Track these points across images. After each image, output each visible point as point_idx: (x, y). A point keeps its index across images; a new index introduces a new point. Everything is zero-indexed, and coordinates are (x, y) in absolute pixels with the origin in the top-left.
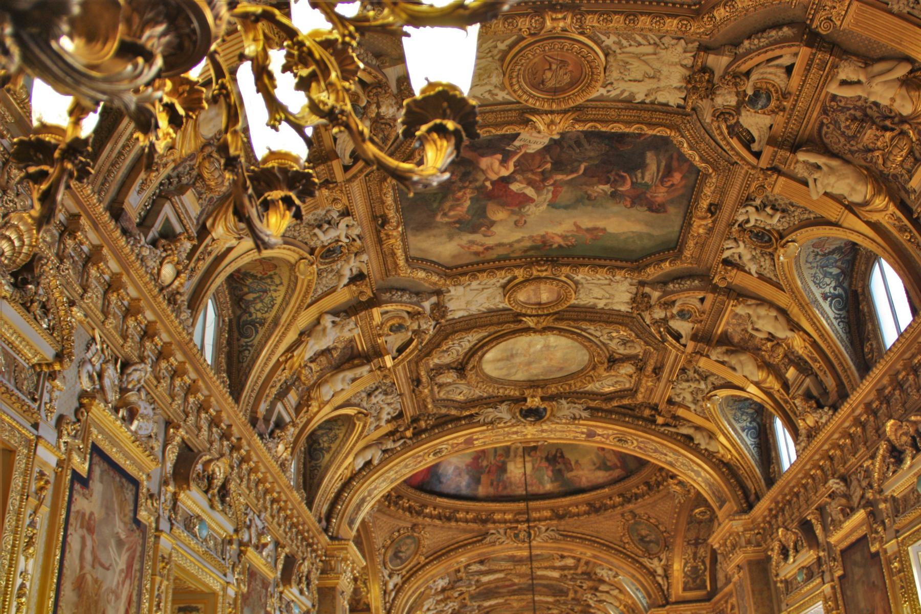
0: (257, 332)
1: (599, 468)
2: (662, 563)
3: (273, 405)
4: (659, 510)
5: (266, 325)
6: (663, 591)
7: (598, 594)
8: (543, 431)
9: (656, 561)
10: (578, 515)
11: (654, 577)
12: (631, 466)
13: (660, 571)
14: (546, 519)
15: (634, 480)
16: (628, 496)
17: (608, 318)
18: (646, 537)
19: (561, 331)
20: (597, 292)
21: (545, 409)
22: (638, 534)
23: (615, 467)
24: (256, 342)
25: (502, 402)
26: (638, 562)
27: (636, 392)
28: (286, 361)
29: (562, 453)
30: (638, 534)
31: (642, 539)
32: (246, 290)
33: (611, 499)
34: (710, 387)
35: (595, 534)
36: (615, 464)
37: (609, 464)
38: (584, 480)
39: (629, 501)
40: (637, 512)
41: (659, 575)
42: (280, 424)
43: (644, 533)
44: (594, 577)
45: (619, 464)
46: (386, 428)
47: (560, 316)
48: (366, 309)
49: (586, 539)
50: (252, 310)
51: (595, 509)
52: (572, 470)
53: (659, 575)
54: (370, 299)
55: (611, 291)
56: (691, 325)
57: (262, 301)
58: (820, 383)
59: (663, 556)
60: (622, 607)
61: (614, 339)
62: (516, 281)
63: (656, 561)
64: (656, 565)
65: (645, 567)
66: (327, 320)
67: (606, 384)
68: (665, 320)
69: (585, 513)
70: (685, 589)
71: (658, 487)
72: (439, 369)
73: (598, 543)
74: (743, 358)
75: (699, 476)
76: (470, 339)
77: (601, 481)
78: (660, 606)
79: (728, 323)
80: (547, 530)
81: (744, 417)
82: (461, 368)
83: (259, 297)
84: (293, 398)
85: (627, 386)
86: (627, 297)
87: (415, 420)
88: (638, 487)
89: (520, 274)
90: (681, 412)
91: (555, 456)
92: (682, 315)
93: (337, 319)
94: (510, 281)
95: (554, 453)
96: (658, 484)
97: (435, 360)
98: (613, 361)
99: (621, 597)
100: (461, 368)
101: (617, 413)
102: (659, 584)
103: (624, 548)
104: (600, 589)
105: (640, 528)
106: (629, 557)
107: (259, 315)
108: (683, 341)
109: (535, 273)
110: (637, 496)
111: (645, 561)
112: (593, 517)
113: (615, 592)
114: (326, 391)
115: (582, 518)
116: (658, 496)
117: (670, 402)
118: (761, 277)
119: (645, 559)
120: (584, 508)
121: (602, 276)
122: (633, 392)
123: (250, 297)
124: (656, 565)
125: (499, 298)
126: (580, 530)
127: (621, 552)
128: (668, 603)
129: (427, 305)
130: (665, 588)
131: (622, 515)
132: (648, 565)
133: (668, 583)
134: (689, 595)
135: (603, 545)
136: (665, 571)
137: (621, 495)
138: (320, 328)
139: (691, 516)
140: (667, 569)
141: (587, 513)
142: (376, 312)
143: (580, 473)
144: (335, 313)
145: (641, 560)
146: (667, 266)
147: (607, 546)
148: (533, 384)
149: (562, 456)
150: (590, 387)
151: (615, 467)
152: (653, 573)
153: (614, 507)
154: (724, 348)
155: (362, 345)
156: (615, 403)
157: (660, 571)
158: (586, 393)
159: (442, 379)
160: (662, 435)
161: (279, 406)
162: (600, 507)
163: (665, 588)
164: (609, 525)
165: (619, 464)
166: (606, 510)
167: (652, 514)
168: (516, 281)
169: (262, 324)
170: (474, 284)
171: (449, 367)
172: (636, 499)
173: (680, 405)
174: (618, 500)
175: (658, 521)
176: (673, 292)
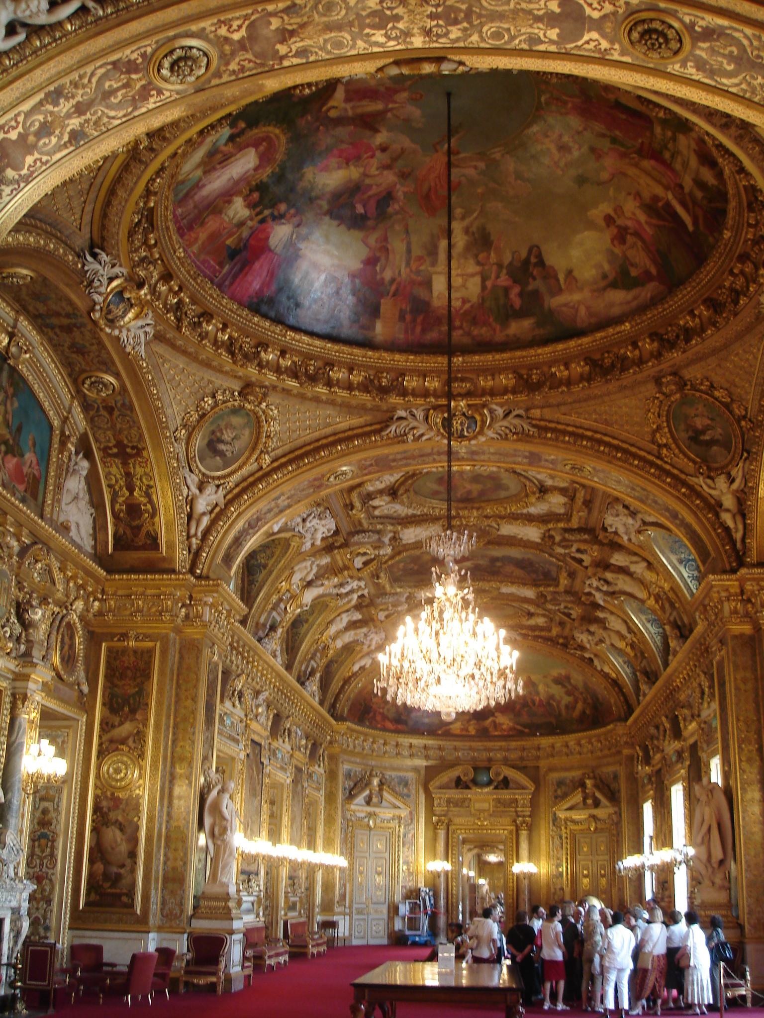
1: (614, 285)
2: (735, 486)
6: (733, 542)
7: (609, 576)
9: (721, 482)
10: (569, 382)
11: (717, 516)
14: (505, 391)
15: (685, 294)
16: (671, 336)
18: (703, 432)
22: (689, 427)
23: (647, 277)
26: (684, 484)
29: (539, 256)
30: (689, 427)
31: (695, 437)
33: (635, 345)
35: (601, 427)
36: (647, 273)
37: (634, 272)
38: (583, 311)
39: (672, 345)
40: (687, 374)
41: (728, 510)
43: (699, 423)
44: (601, 537)
45: (654, 271)
49: (583, 437)
52: (560, 291)
53: (728, 510)
59: (737, 472)
60: (651, 602)
63: (721, 482)
64: (722, 490)
65: (699, 495)
69: (582, 378)
71: (736, 302)
73: (607, 444)
77: (616, 311)
78: (724, 572)
80: (506, 415)
88: (691, 313)
91: (526, 262)
95: (524, 254)
96: (736, 294)
99: (650, 576)
102: (727, 529)
103: (659, 457)
104: (613, 561)
105: (691, 412)
106: (668, 474)
110: (688, 334)
111: (700, 482)
112: (598, 387)
113: (639, 568)
115: (575, 389)
116: (736, 325)
119: (701, 480)
126: (573, 418)
127: (652, 464)
128: (741, 564)
130: (738, 536)
131: (658, 381)
133: (745, 526)
135: (617, 448)
143: (576, 297)
145: (692, 480)
147: (625, 451)
149: (541, 263)
151: (647, 277)
152: (715, 507)
157: (729, 502)
162: (613, 366)
163: (738, 536)
164: (630, 408)
165: (654, 271)
166: (623, 370)
167: (717, 379)
172: (688, 340)
174: (648, 346)
175: (730, 394)
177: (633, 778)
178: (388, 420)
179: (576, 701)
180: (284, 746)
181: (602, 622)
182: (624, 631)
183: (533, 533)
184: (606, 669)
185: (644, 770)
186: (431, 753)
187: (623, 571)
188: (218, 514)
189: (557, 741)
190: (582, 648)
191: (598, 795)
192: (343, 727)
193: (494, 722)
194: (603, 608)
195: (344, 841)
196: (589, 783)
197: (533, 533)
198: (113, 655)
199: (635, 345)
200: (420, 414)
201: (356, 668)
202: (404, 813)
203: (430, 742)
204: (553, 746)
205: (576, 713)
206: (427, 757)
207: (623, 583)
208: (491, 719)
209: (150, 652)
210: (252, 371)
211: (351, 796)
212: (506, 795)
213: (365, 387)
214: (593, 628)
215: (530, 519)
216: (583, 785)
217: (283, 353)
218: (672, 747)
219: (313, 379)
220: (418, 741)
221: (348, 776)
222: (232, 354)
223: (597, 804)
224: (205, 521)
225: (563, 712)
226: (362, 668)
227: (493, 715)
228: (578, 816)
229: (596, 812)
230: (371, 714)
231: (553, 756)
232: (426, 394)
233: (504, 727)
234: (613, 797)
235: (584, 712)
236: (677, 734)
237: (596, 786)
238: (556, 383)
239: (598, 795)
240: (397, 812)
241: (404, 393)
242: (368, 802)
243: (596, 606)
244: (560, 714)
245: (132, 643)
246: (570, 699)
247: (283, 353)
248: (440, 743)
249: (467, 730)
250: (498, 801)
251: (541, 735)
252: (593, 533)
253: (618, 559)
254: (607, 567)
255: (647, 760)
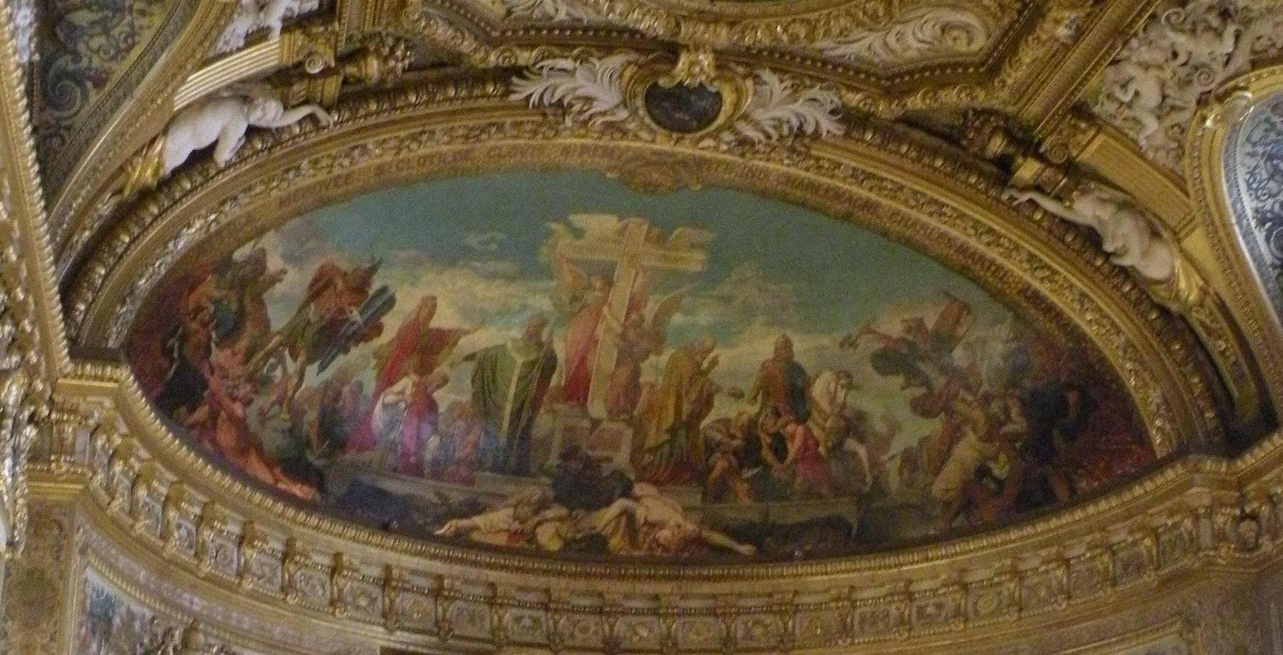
179: (953, 436)
186: (405, 602)
189: (869, 578)
193: (629, 515)
201: (177, 149)
203: (405, 559)
204: (849, 597)
205: (949, 479)
206: (389, 618)
208: (619, 504)
220: (368, 552)
225: (894, 482)
227: (627, 492)
230: (201, 413)
231: (846, 630)
233: (664, 535)
235: (983, 472)
244: (879, 487)
246: (932, 427)
248: (439, 567)
249: (532, 539)
251: (809, 557)
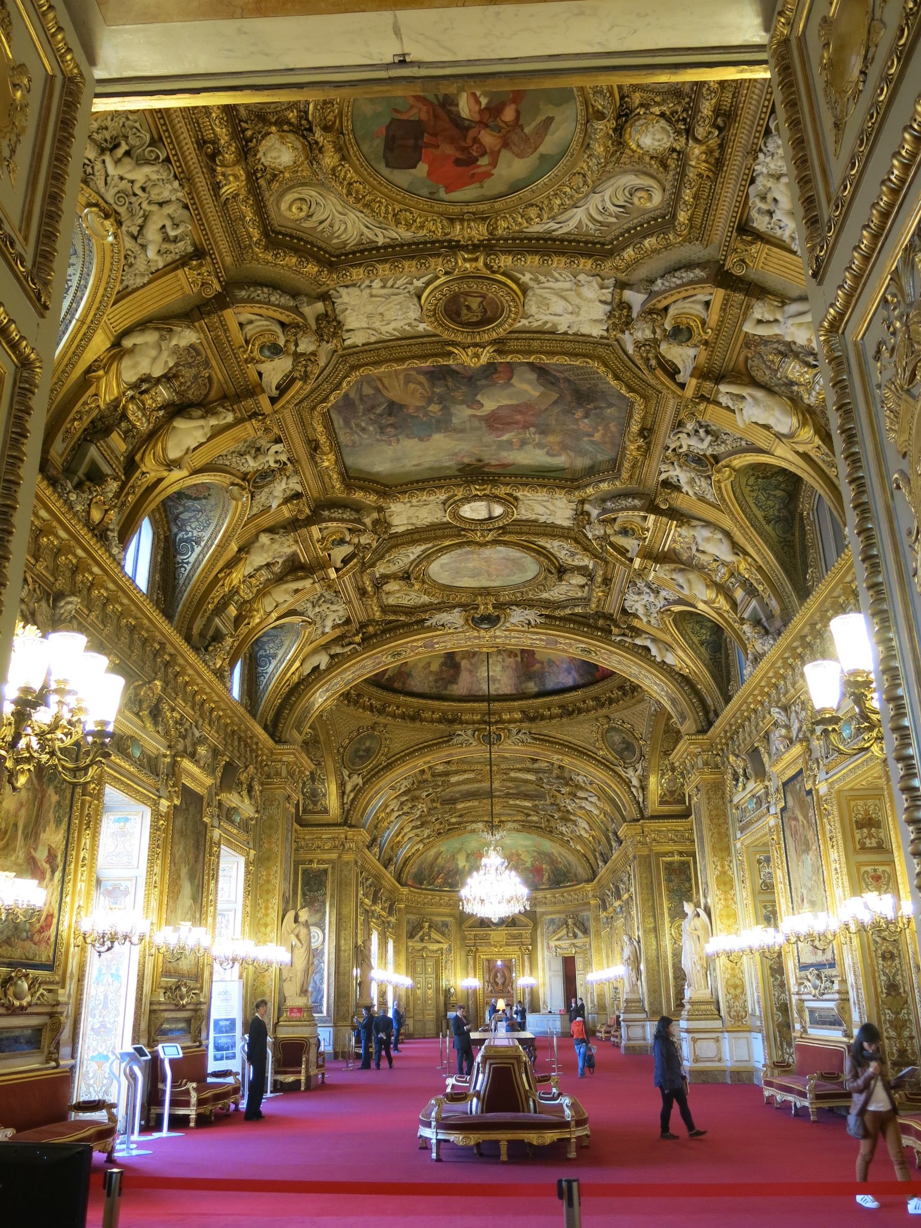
0: (193, 550)
3: (210, 620)
4: (635, 718)
5: (203, 544)
6: (638, 803)
8: (496, 637)
12: (594, 675)
13: (635, 782)
16: (603, 700)
17: (552, 531)
19: (506, 543)
20: (539, 509)
21: (498, 617)
24: (192, 560)
25: (454, 607)
27: (590, 600)
28: (224, 578)
32: (181, 509)
33: (584, 702)
34: (663, 602)
42: (218, 637)
46: (332, 634)
47: (504, 529)
48: (305, 526)
50: (189, 529)
51: (568, 712)
54: (308, 518)
55: (556, 509)
56: (636, 542)
57: (197, 520)
58: (765, 605)
59: (639, 767)
61: (561, 549)
62: (456, 498)
63: (631, 772)
65: (620, 776)
66: (264, 539)
67: (558, 592)
68: (605, 538)
70: (662, 803)
72: (386, 578)
74: (692, 576)
75: (656, 687)
76: (415, 551)
79: (674, 541)
81: (703, 631)
82: (406, 577)
83: (194, 516)
84: (232, 611)
85: (580, 594)
86: (569, 513)
87: (363, 626)
89: (460, 493)
90: (636, 623)
92: (625, 532)
93: (277, 536)
94: (449, 498)
97: (381, 569)
98: (562, 571)
100: (406, 577)
101: (575, 622)
107: (195, 533)
108: (629, 555)
109: (474, 492)
110: (611, 701)
114: (268, 603)
115: (553, 721)
117: (624, 611)
118: (702, 499)
120: (557, 711)
121: (542, 495)
122: (587, 601)
123: (185, 516)
124: (633, 776)
125: (440, 514)
128: (643, 817)
129: (368, 521)
130: (641, 800)
132: (623, 774)
134: (666, 809)
136: (641, 781)
137: (596, 699)
138: (257, 545)
139: (667, 724)
140: (643, 780)
141: (561, 717)
142: (315, 530)
144: (271, 530)
146: (604, 486)
148: (485, 592)
150: (545, 595)
152: (628, 783)
153: (588, 711)
154: (673, 566)
155: (304, 558)
156: (568, 611)
157: (635, 782)
158: (541, 600)
159: (387, 588)
160: (620, 645)
161: (217, 620)
162: (573, 711)
163: (641, 800)
164: (582, 731)
168: (456, 498)
169: (198, 543)
170: (414, 500)
171: (394, 577)
172: (610, 704)
173: (635, 616)
176: (612, 511)
177: (597, 919)
178: (451, 736)
180: (378, 908)
181: (575, 823)
182: (587, 828)
183: (531, 777)
184: (579, 848)
185: (603, 915)
187: (586, 799)
188: (358, 791)
190: (562, 834)
191: (576, 930)
192: (405, 890)
194: (575, 815)
195: (407, 968)
196: (570, 921)
197: (531, 777)
198: (305, 872)
199: (584, 702)
200: (469, 732)
202: (445, 946)
207: (584, 804)
209: (326, 871)
210: (382, 720)
211: (411, 936)
212: (515, 932)
213: (440, 721)
214: (569, 824)
215: (528, 771)
216: (566, 923)
217: (398, 708)
218: (617, 903)
219: (413, 719)
221: (408, 922)
222: (372, 711)
223: (575, 936)
224: (352, 795)
226: (418, 850)
228: (564, 944)
229: (575, 941)
232: (474, 723)
234: (586, 931)
236: (619, 897)
237: (575, 924)
238: (543, 718)
239: (576, 930)
240: (441, 945)
241: (461, 723)
242: (422, 940)
243: (568, 811)
245: (315, 866)
247: (398, 708)
250: (510, 935)
252: (568, 781)
253: (581, 794)
254: (575, 796)
255: (605, 909)
